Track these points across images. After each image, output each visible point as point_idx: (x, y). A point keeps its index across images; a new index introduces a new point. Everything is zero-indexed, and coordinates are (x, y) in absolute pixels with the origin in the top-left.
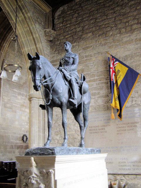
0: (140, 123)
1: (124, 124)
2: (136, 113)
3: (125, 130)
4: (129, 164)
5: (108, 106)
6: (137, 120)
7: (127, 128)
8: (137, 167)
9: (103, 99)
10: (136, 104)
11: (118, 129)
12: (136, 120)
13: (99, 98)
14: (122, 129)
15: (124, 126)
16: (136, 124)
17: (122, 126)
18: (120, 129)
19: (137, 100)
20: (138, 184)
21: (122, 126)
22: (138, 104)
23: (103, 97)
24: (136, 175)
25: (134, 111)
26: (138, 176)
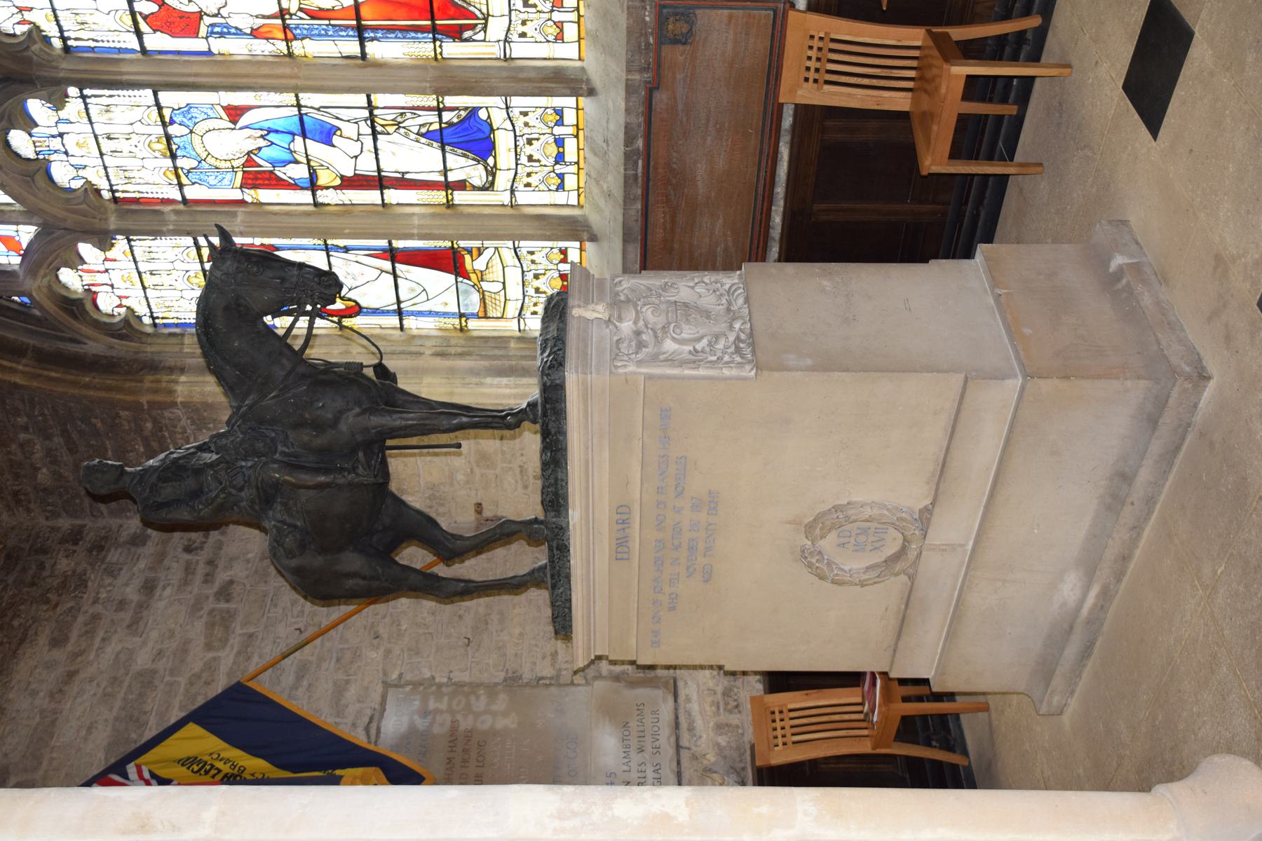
0: (459, 717)
4: (634, 765)
6: (442, 725)
8: (649, 739)
20: (718, 745)
24: (678, 747)
26: (685, 742)
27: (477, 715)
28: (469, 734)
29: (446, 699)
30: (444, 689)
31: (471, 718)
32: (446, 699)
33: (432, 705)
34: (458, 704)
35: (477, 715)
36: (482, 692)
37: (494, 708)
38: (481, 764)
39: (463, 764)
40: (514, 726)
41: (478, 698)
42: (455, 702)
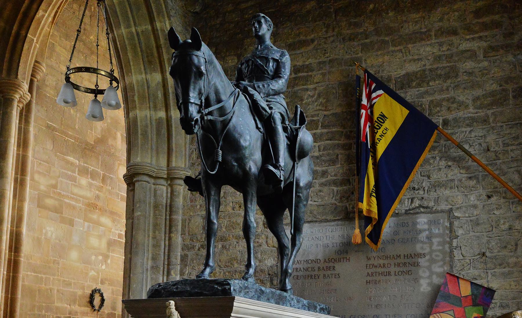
0: (427, 257)
1: (387, 257)
2: (421, 231)
3: (389, 274)
5: (346, 207)
6: (422, 248)
7: (393, 269)
9: (335, 189)
10: (420, 206)
11: (370, 271)
12: (418, 248)
13: (326, 185)
14: (380, 270)
15: (386, 262)
16: (420, 260)
17: (381, 262)
18: (374, 270)
19: (426, 195)
21: (381, 262)
22: (427, 207)
23: (335, 183)
25: (415, 224)
27: (429, 268)
28: (417, 265)
29: (441, 248)
30: (447, 246)
31: (427, 264)
32: (441, 248)
33: (435, 240)
34: (437, 256)
35: (429, 268)
36: (446, 268)
37: (434, 277)
38: (396, 274)
39: (397, 264)
40: (422, 290)
41: (442, 266)
42: (438, 253)
